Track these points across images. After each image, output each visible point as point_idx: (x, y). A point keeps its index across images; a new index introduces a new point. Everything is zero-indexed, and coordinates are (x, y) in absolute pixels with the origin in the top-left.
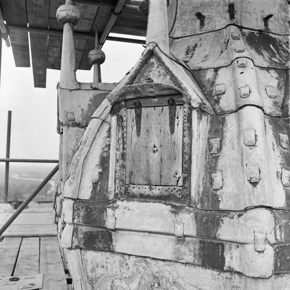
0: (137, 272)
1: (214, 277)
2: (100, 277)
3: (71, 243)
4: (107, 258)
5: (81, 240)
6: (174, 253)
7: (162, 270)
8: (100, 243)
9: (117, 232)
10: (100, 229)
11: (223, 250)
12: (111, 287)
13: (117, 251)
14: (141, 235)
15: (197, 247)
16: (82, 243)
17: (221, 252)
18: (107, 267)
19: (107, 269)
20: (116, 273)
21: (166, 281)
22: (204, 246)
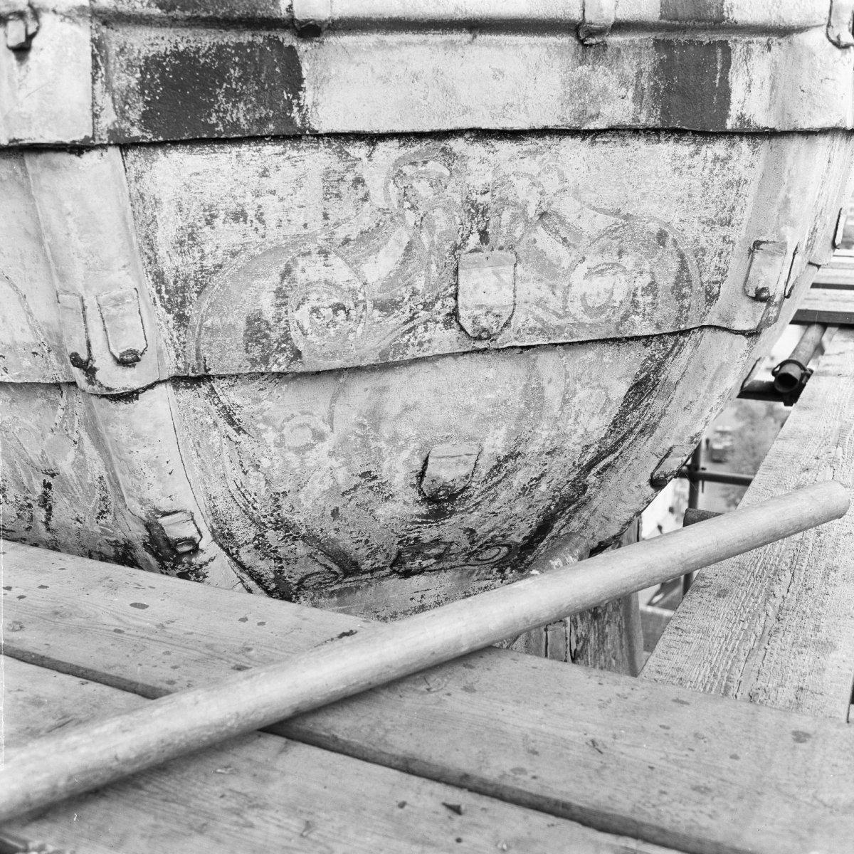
0: (401, 204)
1: (678, 163)
2: (221, 266)
3: (89, 114)
4: (266, 170)
5: (126, 103)
6: (567, 97)
7: (509, 176)
8: (234, 106)
9: (322, 42)
10: (230, 38)
11: (727, 64)
12: (278, 297)
13: (323, 128)
14: (435, 44)
15: (648, 65)
16: (134, 115)
17: (722, 73)
18: (262, 214)
19: (262, 222)
20: (305, 232)
21: (514, 218)
22: (671, 58)
